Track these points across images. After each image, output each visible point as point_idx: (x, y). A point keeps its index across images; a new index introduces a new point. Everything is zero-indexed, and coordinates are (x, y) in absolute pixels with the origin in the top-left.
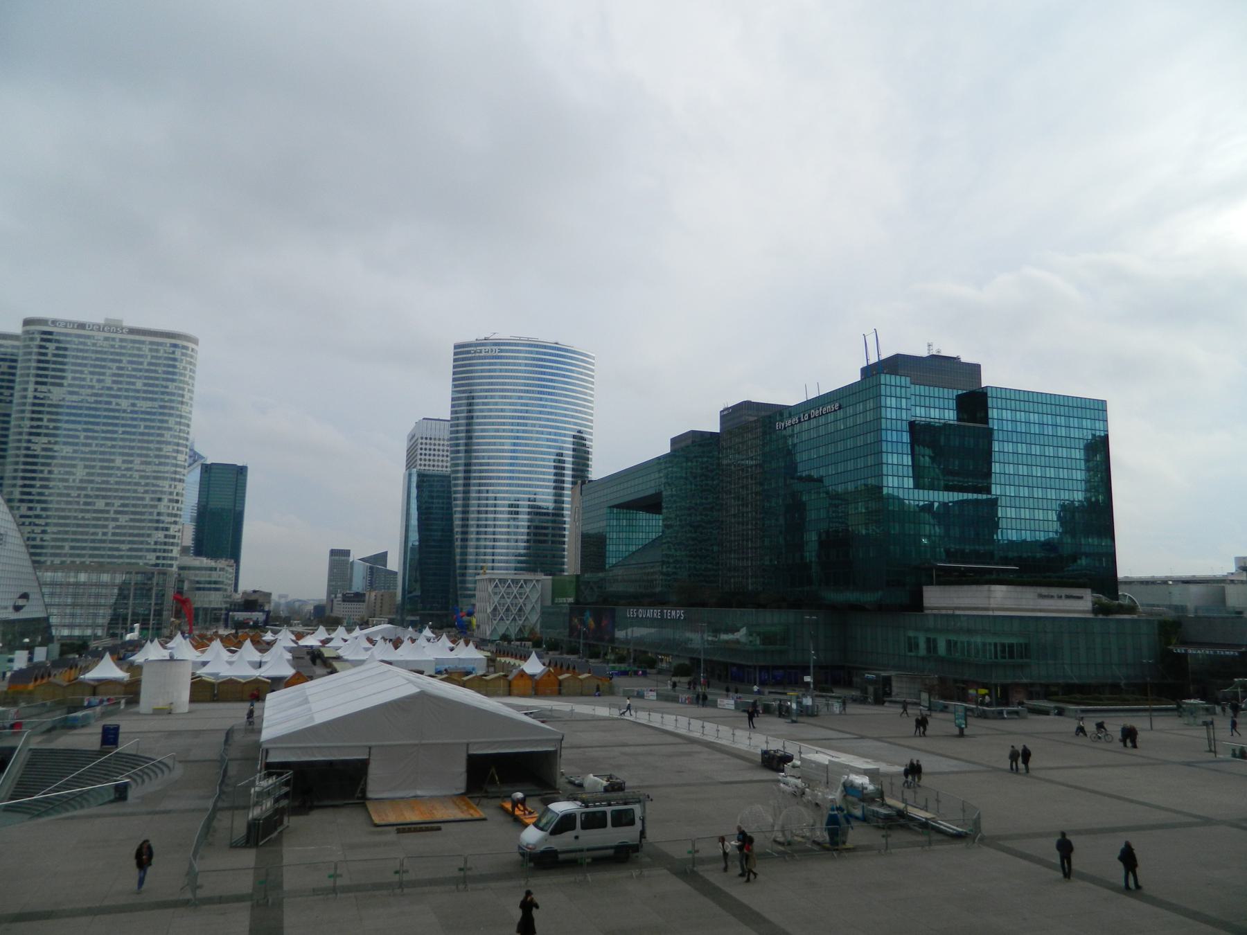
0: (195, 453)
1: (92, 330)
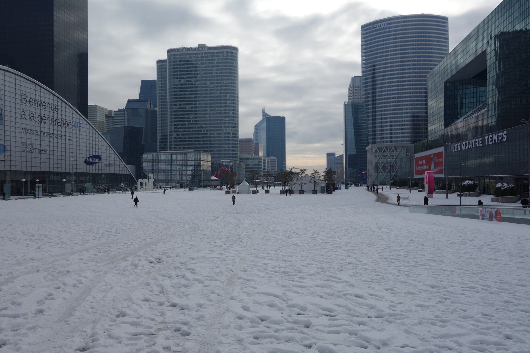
0: (266, 114)
1: (193, 50)
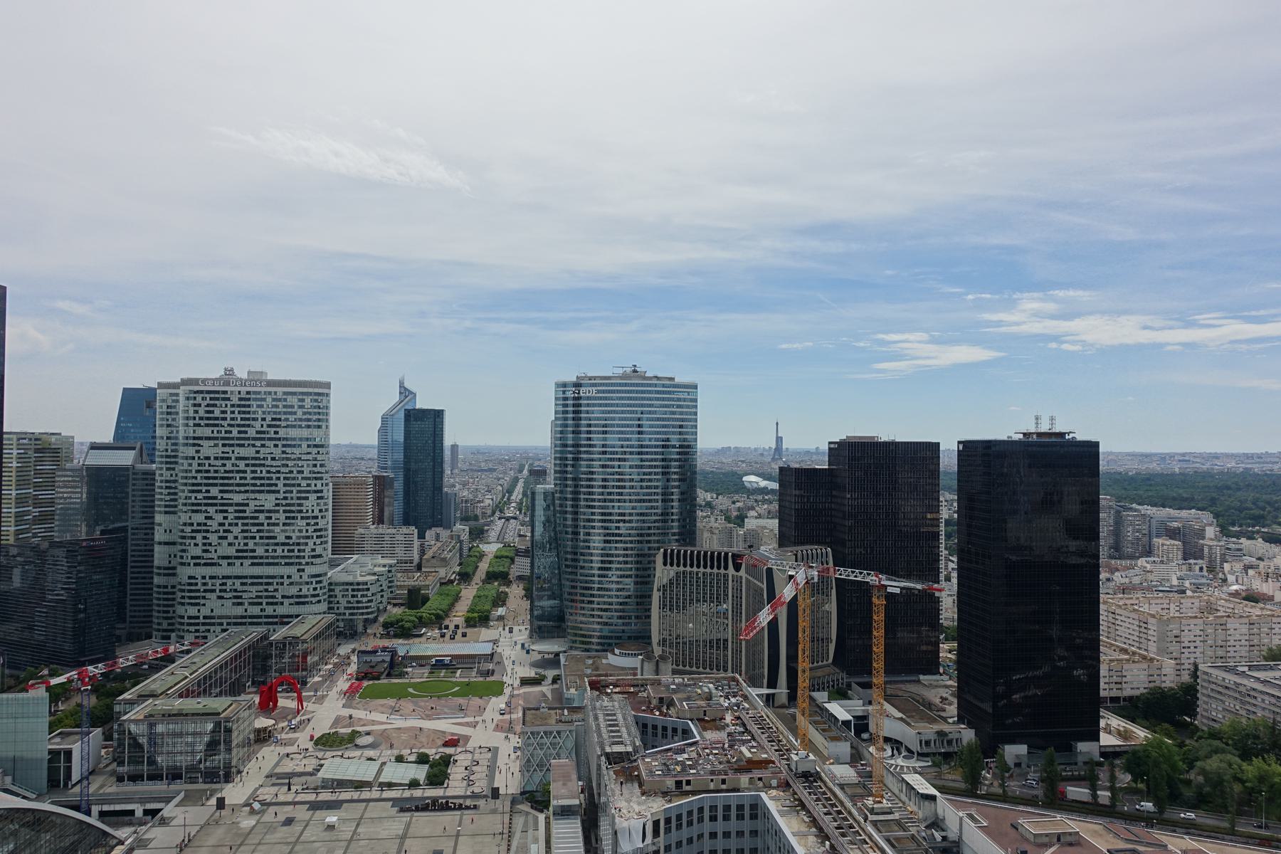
0: (406, 389)
1: (236, 385)
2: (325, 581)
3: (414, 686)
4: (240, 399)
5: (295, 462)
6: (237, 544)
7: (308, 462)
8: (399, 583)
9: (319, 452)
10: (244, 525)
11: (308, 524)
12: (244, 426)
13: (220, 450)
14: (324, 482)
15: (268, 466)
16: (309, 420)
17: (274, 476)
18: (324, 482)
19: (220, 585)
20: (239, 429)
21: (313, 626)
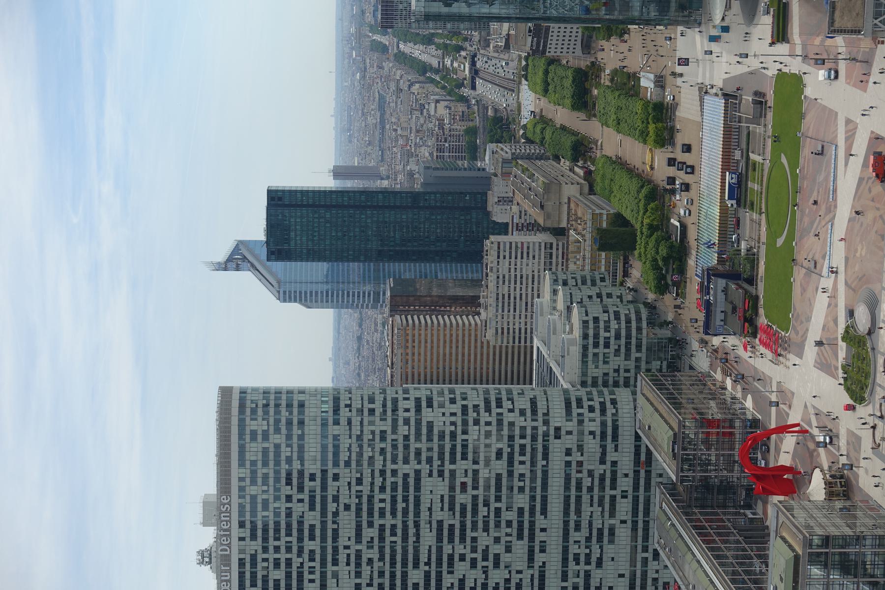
0: (230, 259)
1: (229, 545)
2: (578, 393)
3: (773, 235)
4: (253, 537)
5: (365, 446)
6: (509, 539)
7: (366, 422)
8: (588, 268)
9: (347, 406)
10: (474, 527)
11: (476, 422)
12: (300, 531)
13: (343, 569)
14: (400, 396)
15: (372, 491)
16: (289, 423)
17: (390, 480)
18: (400, 396)
19: (578, 564)
20: (306, 539)
21: (657, 410)
